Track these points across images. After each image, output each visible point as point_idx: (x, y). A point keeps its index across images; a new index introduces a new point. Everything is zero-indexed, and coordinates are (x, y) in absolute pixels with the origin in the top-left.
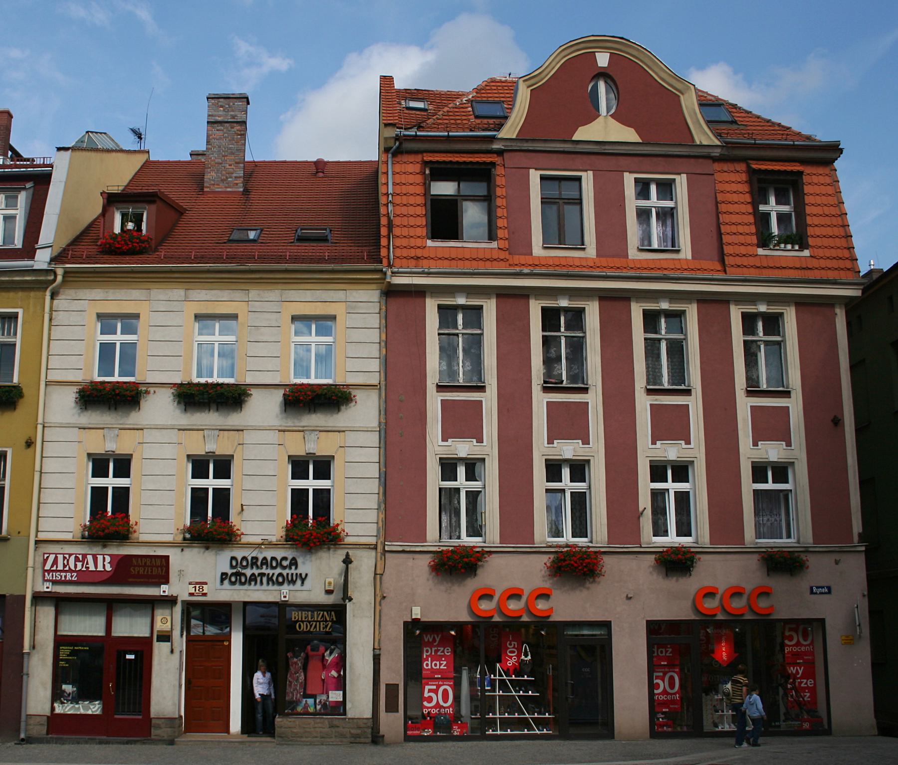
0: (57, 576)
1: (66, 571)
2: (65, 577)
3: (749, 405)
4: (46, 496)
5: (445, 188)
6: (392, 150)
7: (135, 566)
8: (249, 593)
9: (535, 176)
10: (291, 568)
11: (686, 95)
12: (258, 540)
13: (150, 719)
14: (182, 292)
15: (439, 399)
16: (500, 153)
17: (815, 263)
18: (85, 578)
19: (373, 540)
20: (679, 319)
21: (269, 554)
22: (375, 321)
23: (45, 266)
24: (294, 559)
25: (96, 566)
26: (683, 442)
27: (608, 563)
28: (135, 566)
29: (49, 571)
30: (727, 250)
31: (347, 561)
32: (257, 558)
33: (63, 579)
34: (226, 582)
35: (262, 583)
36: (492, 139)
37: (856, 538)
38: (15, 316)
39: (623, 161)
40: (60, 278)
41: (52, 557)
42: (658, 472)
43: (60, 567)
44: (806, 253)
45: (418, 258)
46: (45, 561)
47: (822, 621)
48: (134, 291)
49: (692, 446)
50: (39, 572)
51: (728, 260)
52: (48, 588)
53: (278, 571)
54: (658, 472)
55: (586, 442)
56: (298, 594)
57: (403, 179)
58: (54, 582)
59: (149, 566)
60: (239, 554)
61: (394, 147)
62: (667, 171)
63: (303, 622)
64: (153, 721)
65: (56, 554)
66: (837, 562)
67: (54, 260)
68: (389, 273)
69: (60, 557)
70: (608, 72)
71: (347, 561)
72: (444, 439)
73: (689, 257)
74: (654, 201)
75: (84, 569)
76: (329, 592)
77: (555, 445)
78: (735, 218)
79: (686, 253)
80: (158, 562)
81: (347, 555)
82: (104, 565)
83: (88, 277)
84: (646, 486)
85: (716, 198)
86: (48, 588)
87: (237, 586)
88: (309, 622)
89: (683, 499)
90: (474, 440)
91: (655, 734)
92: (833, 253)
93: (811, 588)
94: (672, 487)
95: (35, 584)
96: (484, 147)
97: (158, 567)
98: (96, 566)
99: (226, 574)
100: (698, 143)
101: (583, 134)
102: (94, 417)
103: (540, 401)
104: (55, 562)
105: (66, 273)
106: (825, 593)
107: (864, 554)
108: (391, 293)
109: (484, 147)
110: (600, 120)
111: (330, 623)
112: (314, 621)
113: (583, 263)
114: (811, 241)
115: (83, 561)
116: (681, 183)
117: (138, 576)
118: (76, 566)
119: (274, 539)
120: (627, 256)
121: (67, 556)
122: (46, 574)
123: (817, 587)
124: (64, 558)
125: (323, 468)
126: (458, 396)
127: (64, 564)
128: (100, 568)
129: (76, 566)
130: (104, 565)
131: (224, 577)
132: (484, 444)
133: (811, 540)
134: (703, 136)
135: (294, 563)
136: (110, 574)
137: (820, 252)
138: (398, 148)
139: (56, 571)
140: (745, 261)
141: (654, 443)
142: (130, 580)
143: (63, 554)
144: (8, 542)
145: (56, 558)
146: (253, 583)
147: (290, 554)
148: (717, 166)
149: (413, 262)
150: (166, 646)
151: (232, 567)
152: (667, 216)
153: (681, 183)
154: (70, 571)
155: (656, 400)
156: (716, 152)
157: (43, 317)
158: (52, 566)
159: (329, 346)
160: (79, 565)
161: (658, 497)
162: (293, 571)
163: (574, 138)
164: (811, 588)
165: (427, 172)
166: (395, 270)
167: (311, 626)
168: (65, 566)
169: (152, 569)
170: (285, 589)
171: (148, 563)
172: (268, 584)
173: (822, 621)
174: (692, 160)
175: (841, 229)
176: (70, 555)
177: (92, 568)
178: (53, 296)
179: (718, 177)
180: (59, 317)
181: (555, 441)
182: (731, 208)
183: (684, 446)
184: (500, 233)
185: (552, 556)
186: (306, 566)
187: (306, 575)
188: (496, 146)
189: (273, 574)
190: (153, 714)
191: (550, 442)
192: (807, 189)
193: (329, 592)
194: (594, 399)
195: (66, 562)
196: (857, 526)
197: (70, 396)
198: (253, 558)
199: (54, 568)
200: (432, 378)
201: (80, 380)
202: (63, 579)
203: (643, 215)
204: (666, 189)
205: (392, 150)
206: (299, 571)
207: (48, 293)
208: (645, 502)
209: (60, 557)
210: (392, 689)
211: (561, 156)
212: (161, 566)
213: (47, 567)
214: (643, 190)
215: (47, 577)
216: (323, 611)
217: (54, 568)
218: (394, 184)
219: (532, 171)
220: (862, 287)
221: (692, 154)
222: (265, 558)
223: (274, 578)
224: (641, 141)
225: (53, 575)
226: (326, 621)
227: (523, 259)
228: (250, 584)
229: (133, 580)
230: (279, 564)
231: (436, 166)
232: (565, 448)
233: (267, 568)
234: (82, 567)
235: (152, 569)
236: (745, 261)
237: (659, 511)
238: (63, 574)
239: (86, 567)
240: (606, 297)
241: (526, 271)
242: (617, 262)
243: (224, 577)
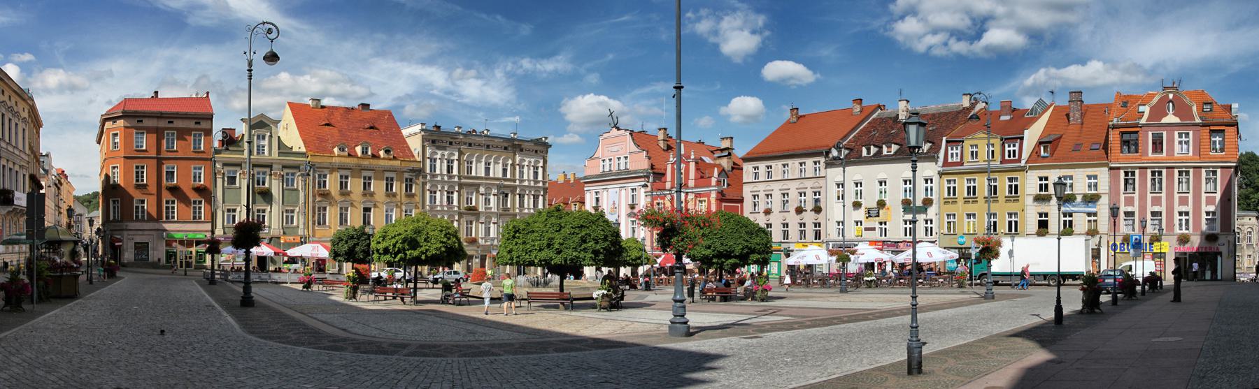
4: (1028, 223)
9: (1150, 134)
17: (1226, 156)
22: (1107, 176)
31: (1101, 238)
42: (1180, 214)
44: (1224, 153)
54: (1180, 214)
67: (1026, 163)
71: (1101, 238)
72: (1125, 206)
74: (1184, 139)
78: (1205, 144)
79: (1191, 154)
84: (1177, 217)
89: (1187, 221)
94: (1184, 218)
101: (1165, 120)
103: (1149, 196)
116: (1191, 133)
120: (1174, 155)
125: (1095, 214)
140: (1206, 156)
152: (1187, 143)
153: (1191, 133)
159: (1097, 183)
179: (1202, 131)
182: (1204, 140)
184: (1140, 151)
197: (1031, 198)
203: (1180, 143)
204: (1187, 135)
208: (1176, 222)
214: (1180, 135)
227: (1146, 158)
236: (1206, 156)
237: (1180, 225)
242: (1171, 157)
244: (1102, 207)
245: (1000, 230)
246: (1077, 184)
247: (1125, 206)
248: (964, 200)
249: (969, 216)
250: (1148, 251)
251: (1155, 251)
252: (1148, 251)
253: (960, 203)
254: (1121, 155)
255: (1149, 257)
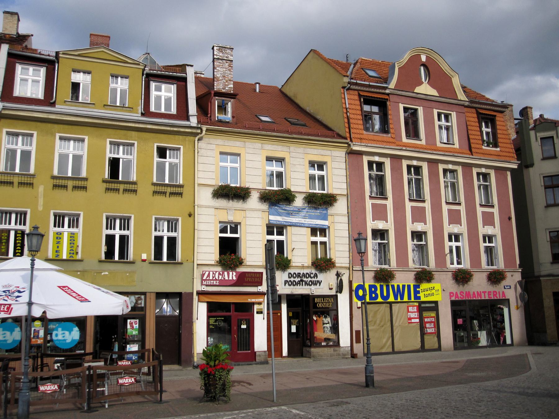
0: (209, 283)
1: (214, 280)
2: (213, 283)
3: (481, 211)
5: (367, 108)
6: (346, 88)
7: (247, 277)
8: (297, 290)
10: (314, 278)
11: (454, 78)
12: (300, 265)
13: (255, 353)
14: (260, 145)
15: (371, 202)
16: (388, 94)
18: (223, 283)
19: (348, 265)
20: (453, 173)
21: (305, 271)
23: (195, 125)
24: (316, 274)
25: (229, 277)
26: (459, 225)
27: (436, 275)
28: (247, 277)
29: (205, 280)
30: (473, 145)
31: (338, 275)
32: (300, 274)
33: (212, 284)
34: (287, 284)
35: (302, 285)
36: (386, 88)
37: (518, 266)
38: (178, 149)
39: (434, 104)
40: (204, 132)
41: (207, 273)
43: (211, 278)
44: (498, 149)
45: (361, 139)
46: (203, 275)
47: (508, 300)
48: (237, 142)
49: (462, 227)
50: (200, 280)
51: (473, 150)
52: (204, 288)
53: (309, 279)
55: (425, 224)
56: (318, 290)
57: (353, 102)
58: (207, 285)
59: (253, 277)
60: (292, 271)
61: (348, 87)
62: (449, 110)
63: (320, 303)
64: (257, 354)
65: (209, 271)
66: (512, 276)
68: (352, 145)
69: (211, 273)
70: (425, 64)
72: (373, 221)
73: (458, 147)
74: (443, 122)
75: (223, 279)
76: (331, 289)
77: (414, 225)
79: (457, 146)
80: (258, 276)
81: (337, 272)
82: (232, 277)
83: (216, 133)
84: (447, 244)
85: (466, 123)
86: (204, 288)
87: (292, 286)
88: (322, 303)
90: (385, 221)
91: (456, 348)
92: (507, 150)
93: (504, 286)
95: (198, 287)
96: (381, 91)
97: (257, 278)
98: (229, 277)
99: (287, 281)
100: (459, 99)
102: (222, 203)
103: (409, 205)
104: (209, 275)
105: (207, 130)
106: (509, 288)
107: (520, 273)
108: (351, 153)
109: (383, 91)
110: (424, 85)
111: (331, 304)
112: (324, 302)
113: (421, 147)
114: (500, 144)
115: (222, 275)
116: (454, 115)
117: (249, 282)
118: (219, 277)
119: (306, 265)
121: (215, 272)
122: (204, 281)
123: (506, 286)
124: (213, 273)
125: (323, 231)
126: (377, 202)
127: (213, 276)
128: (231, 278)
129: (219, 277)
130: (232, 277)
131: (286, 282)
132: (389, 223)
133: (503, 267)
134: (461, 96)
135: (316, 275)
136: (235, 281)
137: (503, 149)
138: (350, 87)
139: (209, 280)
141: (449, 225)
142: (244, 284)
143: (213, 271)
144: (182, 265)
145: (209, 273)
146: (299, 285)
147: (314, 271)
148: (466, 109)
149: (359, 140)
150: (261, 316)
151: (289, 277)
153: (454, 115)
154: (216, 280)
155: (449, 207)
156: (467, 104)
157: (194, 150)
158: (207, 277)
160: (220, 277)
161: (451, 248)
162: (315, 279)
163: (415, 91)
164: (504, 286)
165: (362, 100)
166: (354, 143)
167: (323, 305)
168: (213, 277)
169: (255, 279)
170: (313, 287)
171: (253, 276)
172: (305, 285)
173: (508, 300)
174: (457, 106)
175: (509, 140)
176: (216, 272)
177: (227, 278)
178: (199, 140)
180: (202, 152)
181: (415, 223)
183: (460, 227)
184: (391, 131)
185: (416, 272)
186: (321, 277)
187: (321, 281)
188: (387, 91)
189: (307, 281)
190: (256, 349)
191: (413, 223)
192: (498, 123)
193: (331, 289)
194: (427, 205)
195: (214, 275)
196: (518, 262)
198: (298, 273)
199: (208, 279)
200: (367, 194)
201: (214, 184)
202: (212, 284)
203: (440, 127)
204: (447, 117)
205: (346, 88)
206: (318, 279)
207: (197, 139)
208: (447, 251)
209: (211, 273)
210: (358, 332)
211: (411, 98)
212: (259, 277)
213: (204, 278)
215: (204, 283)
216: (328, 298)
217: (208, 279)
218: (349, 104)
219: (400, 104)
220: (517, 165)
221: (459, 104)
222: (304, 274)
223: (308, 282)
224: (438, 95)
225: (207, 282)
226: (329, 302)
228: (297, 285)
229: (246, 284)
230: (310, 276)
231: (365, 97)
232: (418, 226)
233: (304, 278)
234: (222, 278)
235: (255, 279)
238: (212, 282)
239: (224, 278)
240: (433, 163)
241: (404, 148)
243: (286, 282)
244: (337, 219)
245: (137, 252)
246: (294, 175)
247: (373, 221)
248: (52, 182)
249: (59, 220)
250: (413, 299)
251: (423, 299)
252: (413, 299)
253: (41, 189)
254: (365, 132)
255: (415, 309)
